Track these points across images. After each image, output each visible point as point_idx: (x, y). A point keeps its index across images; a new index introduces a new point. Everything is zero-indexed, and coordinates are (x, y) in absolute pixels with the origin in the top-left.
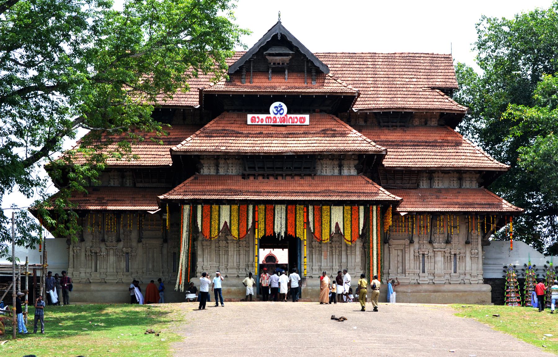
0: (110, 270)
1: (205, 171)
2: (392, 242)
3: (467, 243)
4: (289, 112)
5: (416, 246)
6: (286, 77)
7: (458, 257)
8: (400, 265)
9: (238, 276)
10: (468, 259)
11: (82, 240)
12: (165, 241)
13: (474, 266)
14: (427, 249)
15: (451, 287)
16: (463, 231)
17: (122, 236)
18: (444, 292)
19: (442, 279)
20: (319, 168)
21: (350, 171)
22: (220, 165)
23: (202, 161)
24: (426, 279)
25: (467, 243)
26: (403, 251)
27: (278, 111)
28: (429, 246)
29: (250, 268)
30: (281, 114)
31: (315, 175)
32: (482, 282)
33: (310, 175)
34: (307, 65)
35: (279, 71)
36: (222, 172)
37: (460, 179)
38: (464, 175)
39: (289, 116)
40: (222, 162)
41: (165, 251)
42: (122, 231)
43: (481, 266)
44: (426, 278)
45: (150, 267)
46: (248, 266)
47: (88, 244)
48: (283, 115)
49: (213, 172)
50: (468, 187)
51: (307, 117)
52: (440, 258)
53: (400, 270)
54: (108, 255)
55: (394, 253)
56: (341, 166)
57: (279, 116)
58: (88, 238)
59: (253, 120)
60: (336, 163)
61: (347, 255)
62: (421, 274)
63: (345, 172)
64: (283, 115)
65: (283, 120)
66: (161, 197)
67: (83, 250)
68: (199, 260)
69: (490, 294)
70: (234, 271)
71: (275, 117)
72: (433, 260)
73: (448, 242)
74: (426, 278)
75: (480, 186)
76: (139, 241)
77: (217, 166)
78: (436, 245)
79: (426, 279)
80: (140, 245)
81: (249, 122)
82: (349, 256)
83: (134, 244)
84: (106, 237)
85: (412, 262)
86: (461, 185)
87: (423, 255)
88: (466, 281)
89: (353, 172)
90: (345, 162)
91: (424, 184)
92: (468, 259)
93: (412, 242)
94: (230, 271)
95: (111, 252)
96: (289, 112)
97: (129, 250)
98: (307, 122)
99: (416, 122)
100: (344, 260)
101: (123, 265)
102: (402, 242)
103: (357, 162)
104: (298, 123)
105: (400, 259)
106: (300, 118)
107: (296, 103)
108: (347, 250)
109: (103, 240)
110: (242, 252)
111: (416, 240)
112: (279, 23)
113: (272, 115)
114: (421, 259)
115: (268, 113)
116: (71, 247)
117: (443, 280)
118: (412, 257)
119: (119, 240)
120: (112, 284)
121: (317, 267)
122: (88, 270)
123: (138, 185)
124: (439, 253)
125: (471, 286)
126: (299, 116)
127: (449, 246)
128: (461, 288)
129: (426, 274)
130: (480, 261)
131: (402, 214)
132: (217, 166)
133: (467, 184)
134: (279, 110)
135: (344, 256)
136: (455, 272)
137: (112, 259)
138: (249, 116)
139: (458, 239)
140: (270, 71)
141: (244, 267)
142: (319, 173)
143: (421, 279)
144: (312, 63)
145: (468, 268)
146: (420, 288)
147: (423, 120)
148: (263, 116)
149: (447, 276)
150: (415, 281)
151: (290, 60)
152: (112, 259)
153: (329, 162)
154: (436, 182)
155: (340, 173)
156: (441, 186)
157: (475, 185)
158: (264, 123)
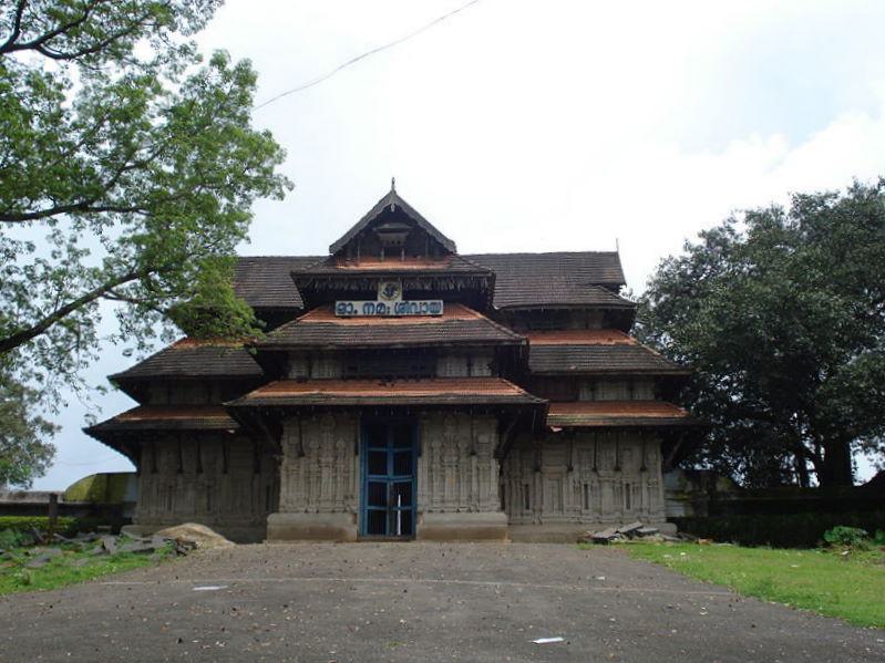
1: (294, 374)
3: (643, 469)
5: (577, 475)
6: (403, 258)
7: (631, 487)
10: (644, 491)
12: (257, 471)
13: (654, 500)
14: (590, 478)
16: (637, 452)
21: (481, 370)
31: (436, 377)
32: (664, 520)
33: (429, 377)
34: (429, 243)
35: (392, 253)
36: (315, 375)
37: (631, 389)
46: (346, 497)
52: (607, 491)
53: (556, 506)
55: (547, 483)
56: (470, 365)
61: (478, 482)
63: (476, 372)
70: (328, 505)
72: (598, 493)
73: (617, 469)
75: (656, 397)
82: (482, 484)
84: (184, 467)
87: (586, 486)
89: (487, 373)
91: (585, 395)
92: (644, 491)
93: (570, 469)
99: (576, 325)
100: (475, 489)
101: (205, 501)
102: (557, 469)
103: (491, 360)
105: (556, 491)
107: (414, 289)
108: (478, 474)
111: (576, 467)
112: (393, 192)
114: (583, 491)
119: (200, 471)
124: (606, 483)
127: (619, 474)
129: (590, 510)
130: (661, 493)
133: (640, 395)
135: (474, 484)
136: (628, 507)
137: (191, 494)
139: (630, 465)
140: (383, 253)
142: (440, 373)
144: (434, 238)
145: (645, 503)
149: (618, 514)
151: (408, 237)
152: (191, 494)
154: (600, 392)
156: (606, 398)
157: (650, 397)
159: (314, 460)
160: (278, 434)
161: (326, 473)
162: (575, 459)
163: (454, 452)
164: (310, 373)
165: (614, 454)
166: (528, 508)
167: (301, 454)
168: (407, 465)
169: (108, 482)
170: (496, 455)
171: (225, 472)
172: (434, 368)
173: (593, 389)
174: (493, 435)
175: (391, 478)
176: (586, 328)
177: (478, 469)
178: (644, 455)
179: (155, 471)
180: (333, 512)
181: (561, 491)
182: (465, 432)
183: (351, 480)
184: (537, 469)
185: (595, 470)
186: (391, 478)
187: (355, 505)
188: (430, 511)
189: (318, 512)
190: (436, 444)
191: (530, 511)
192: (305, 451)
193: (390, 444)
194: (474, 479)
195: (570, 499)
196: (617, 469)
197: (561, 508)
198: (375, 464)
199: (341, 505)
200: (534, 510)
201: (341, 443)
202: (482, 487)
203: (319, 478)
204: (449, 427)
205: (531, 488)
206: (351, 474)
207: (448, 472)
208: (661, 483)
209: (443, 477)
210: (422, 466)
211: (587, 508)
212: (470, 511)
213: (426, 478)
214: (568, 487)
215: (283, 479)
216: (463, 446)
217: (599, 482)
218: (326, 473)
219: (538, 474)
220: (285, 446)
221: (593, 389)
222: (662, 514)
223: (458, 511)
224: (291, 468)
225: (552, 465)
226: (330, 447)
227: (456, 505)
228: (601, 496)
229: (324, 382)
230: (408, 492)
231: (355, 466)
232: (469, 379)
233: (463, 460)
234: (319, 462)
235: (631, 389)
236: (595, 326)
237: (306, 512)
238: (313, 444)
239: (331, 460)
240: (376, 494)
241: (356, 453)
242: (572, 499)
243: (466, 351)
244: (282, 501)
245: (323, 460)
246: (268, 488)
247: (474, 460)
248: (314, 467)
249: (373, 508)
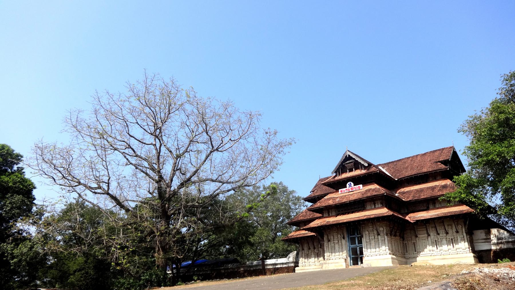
2: (418, 236)
4: (354, 185)
11: (303, 249)
27: (350, 185)
35: (351, 170)
36: (330, 215)
49: (327, 215)
59: (341, 192)
63: (377, 206)
89: (380, 205)
90: (376, 202)
96: (354, 185)
107: (357, 180)
113: (348, 188)
119: (314, 248)
126: (357, 186)
134: (350, 186)
138: (340, 190)
148: (344, 189)
161: (337, 246)
163: (373, 235)
164: (329, 215)
176: (435, 179)
179: (303, 249)
184: (416, 236)
193: (356, 234)
198: (353, 241)
203: (335, 248)
210: (364, 240)
216: (375, 232)
218: (337, 246)
233: (376, 237)
238: (332, 237)
247: (379, 237)
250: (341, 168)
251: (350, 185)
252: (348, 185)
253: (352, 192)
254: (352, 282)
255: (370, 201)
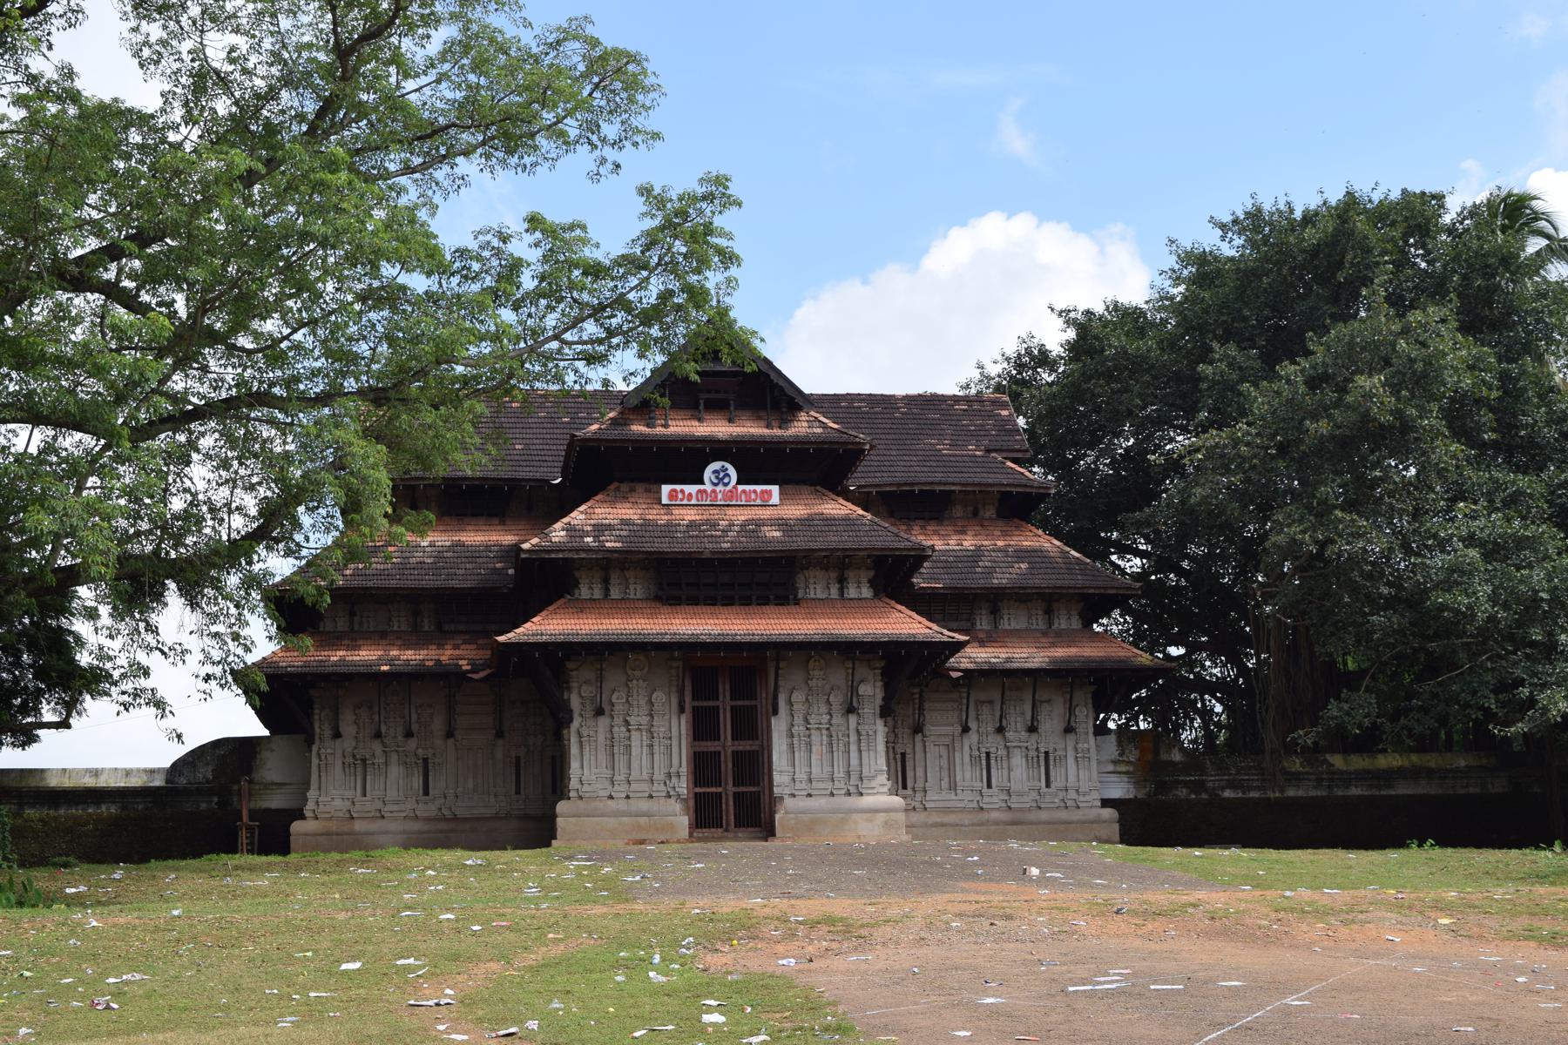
0: (392, 794)
1: (584, 592)
2: (930, 729)
3: (1069, 730)
5: (973, 737)
8: (945, 774)
9: (651, 797)
10: (1071, 761)
11: (337, 735)
12: (499, 735)
14: (993, 743)
15: (1043, 816)
17: (415, 727)
18: (1031, 823)
19: (1025, 799)
20: (800, 584)
22: (612, 581)
23: (577, 574)
24: (995, 800)
25: (1069, 730)
26: (951, 748)
27: (719, 477)
28: (999, 738)
29: (674, 780)
30: (726, 485)
36: (615, 593)
38: (1055, 605)
39: (741, 488)
40: (615, 578)
41: (499, 754)
42: (414, 717)
43: (1095, 774)
44: (994, 798)
45: (471, 784)
46: (669, 776)
47: (347, 744)
48: (729, 487)
49: (598, 594)
50: (1063, 626)
51: (775, 489)
52: (1018, 760)
53: (945, 784)
54: (386, 764)
55: (933, 751)
56: (842, 581)
57: (720, 488)
58: (348, 729)
60: (833, 575)
62: (985, 790)
63: (852, 592)
64: (729, 487)
65: (732, 494)
66: (501, 639)
67: (339, 754)
68: (574, 765)
69: (1116, 826)
70: (645, 787)
71: (714, 491)
72: (1005, 765)
73: (1032, 729)
74: (994, 798)
76: (450, 734)
77: (606, 582)
78: (1010, 735)
79: (995, 800)
80: (450, 742)
81: (665, 500)
83: (439, 742)
84: (383, 729)
85: (968, 767)
86: (1050, 624)
87: (988, 754)
88: (1069, 803)
89: (866, 592)
90: (850, 574)
91: (983, 623)
92: (1071, 761)
94: (634, 786)
95: (394, 757)
96: (739, 483)
97: (430, 753)
98: (775, 499)
99: (958, 511)
100: (854, 761)
101: (417, 782)
103: (871, 573)
104: (759, 502)
105: (944, 762)
106: (763, 492)
107: (756, 463)
109: (378, 735)
110: (656, 748)
111: (973, 725)
113: (708, 487)
115: (702, 483)
116: (315, 748)
117: (1028, 800)
118: (967, 759)
119: (409, 734)
120: (396, 819)
121: (805, 776)
122: (349, 794)
123: (446, 628)
124: (1017, 751)
125: (1080, 812)
126: (759, 488)
127: (1034, 737)
128: (1063, 815)
129: (995, 789)
130: (1094, 764)
131: (955, 675)
132: (606, 582)
133: (1062, 623)
134: (721, 478)
136: (1048, 786)
137: (395, 771)
139: (1051, 722)
141: (662, 777)
143: (986, 799)
145: (1072, 778)
146: (985, 816)
147: (970, 509)
149: (1034, 795)
150: (975, 805)
153: (820, 574)
155: (842, 594)
156: (1014, 625)
158: (694, 502)
159: (618, 721)
160: (561, 679)
162: (972, 713)
163: (823, 709)
164: (607, 591)
165: (1028, 708)
166: (905, 787)
167: (599, 712)
168: (751, 726)
169: (229, 755)
170: (885, 712)
171: (450, 734)
172: (795, 590)
173: (995, 612)
174: (879, 684)
175: (726, 745)
177: (858, 733)
178: (1071, 711)
179: (337, 735)
180: (651, 797)
181: (955, 761)
182: (838, 677)
183: (675, 750)
184: (918, 729)
185: (1000, 730)
186: (726, 745)
187: (683, 786)
188: (793, 795)
189: (628, 797)
190: (798, 697)
191: (909, 792)
192: (606, 708)
194: (853, 748)
195: (968, 775)
196: (1032, 729)
197: (953, 787)
198: (703, 726)
199: (662, 787)
200: (914, 790)
201: (659, 697)
202: (865, 761)
204: (816, 673)
205: (909, 757)
206: (675, 742)
207: (815, 737)
208: (1093, 751)
209: (809, 744)
210: (778, 726)
211: (989, 786)
212: (849, 794)
213: (785, 747)
214: (963, 757)
215: (574, 750)
216: (837, 699)
217: (1007, 748)
219: (919, 737)
220: (575, 702)
221: (995, 612)
222: (1096, 795)
223: (832, 794)
224: (585, 732)
225: (940, 725)
226: (643, 702)
227: (829, 785)
228: (1009, 769)
229: (625, 606)
230: (754, 767)
231: (676, 729)
232: (843, 604)
233: (837, 720)
234: (627, 723)
235: (1049, 612)
236: (988, 515)
237: (611, 797)
239: (645, 720)
240: (703, 768)
241: (682, 710)
242: (968, 775)
243: (839, 564)
244: (574, 784)
245: (633, 720)
246: (518, 759)
247: (853, 719)
248: (620, 731)
249: (698, 790)
250: (671, 389)
251: (719, 477)
252: (708, 473)
253: (724, 507)
254: (1305, 893)
255: (826, 569)
